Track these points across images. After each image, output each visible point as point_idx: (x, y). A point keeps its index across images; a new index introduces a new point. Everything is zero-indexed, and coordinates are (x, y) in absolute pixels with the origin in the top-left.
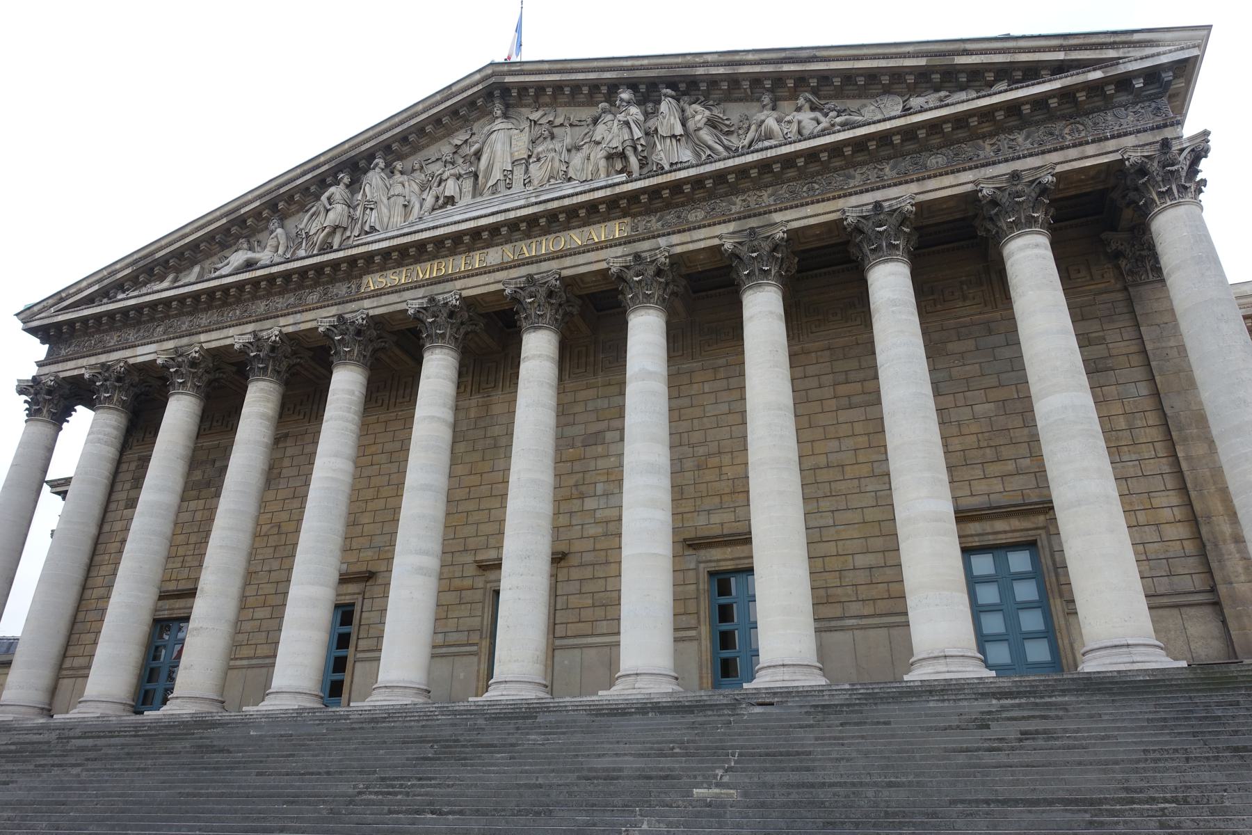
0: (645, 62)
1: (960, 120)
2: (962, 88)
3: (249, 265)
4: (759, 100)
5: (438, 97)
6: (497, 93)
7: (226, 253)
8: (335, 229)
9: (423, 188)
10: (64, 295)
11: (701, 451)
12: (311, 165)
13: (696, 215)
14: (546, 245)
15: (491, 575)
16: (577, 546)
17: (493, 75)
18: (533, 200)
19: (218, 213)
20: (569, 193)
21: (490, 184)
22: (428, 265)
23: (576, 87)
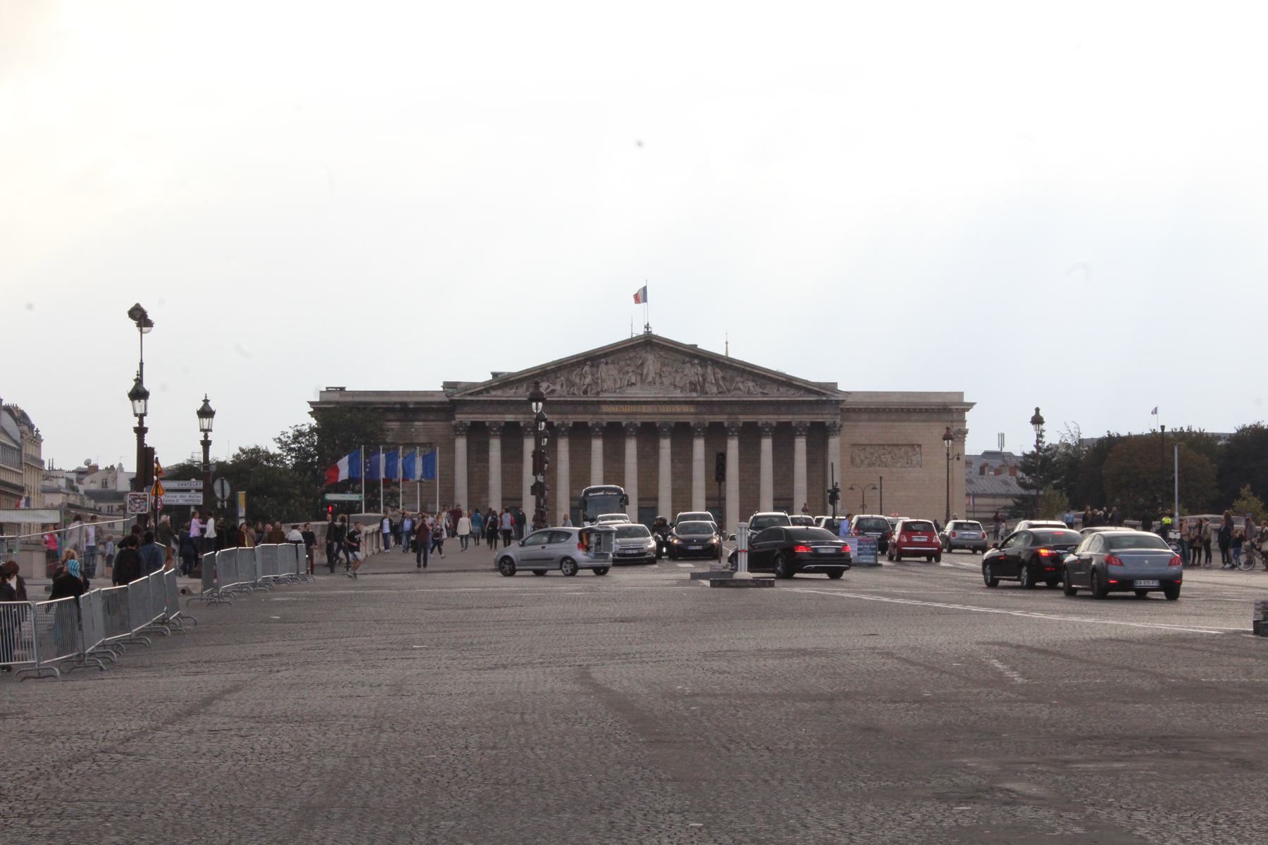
3: (553, 391)
9: (619, 372)
12: (577, 356)
13: (716, 409)
14: (668, 409)
20: (678, 394)
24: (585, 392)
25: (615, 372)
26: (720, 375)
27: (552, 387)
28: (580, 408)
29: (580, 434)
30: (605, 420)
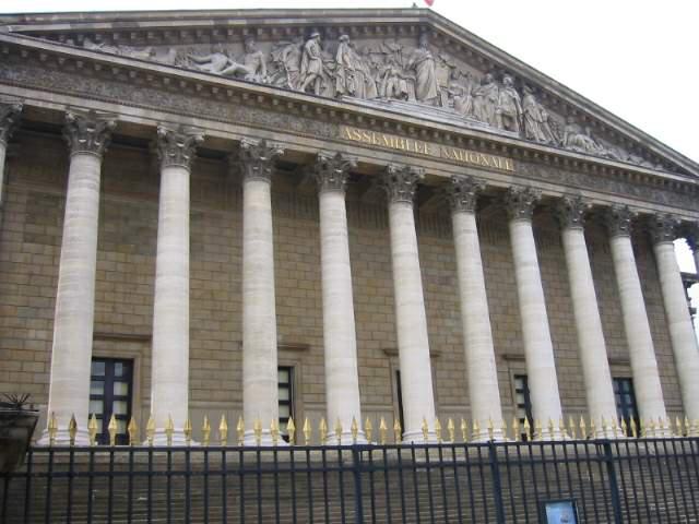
0: (521, 65)
1: (651, 177)
2: (646, 159)
4: (566, 117)
5: (392, 12)
6: (424, 29)
7: (197, 47)
8: (318, 76)
9: (374, 70)
10: (28, 19)
11: (504, 303)
13: (544, 173)
15: (393, 359)
16: (444, 349)
17: (427, 16)
18: (470, 127)
19: (208, 14)
21: (430, 96)
22: (392, 137)
23: (475, 54)
24: (310, 90)
25: (366, 69)
26: (545, 114)
27: (235, 66)
28: (298, 125)
29: (296, 185)
30: (356, 156)
